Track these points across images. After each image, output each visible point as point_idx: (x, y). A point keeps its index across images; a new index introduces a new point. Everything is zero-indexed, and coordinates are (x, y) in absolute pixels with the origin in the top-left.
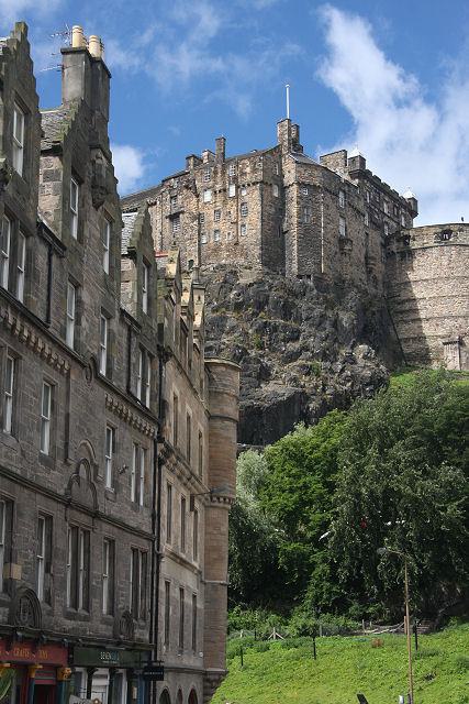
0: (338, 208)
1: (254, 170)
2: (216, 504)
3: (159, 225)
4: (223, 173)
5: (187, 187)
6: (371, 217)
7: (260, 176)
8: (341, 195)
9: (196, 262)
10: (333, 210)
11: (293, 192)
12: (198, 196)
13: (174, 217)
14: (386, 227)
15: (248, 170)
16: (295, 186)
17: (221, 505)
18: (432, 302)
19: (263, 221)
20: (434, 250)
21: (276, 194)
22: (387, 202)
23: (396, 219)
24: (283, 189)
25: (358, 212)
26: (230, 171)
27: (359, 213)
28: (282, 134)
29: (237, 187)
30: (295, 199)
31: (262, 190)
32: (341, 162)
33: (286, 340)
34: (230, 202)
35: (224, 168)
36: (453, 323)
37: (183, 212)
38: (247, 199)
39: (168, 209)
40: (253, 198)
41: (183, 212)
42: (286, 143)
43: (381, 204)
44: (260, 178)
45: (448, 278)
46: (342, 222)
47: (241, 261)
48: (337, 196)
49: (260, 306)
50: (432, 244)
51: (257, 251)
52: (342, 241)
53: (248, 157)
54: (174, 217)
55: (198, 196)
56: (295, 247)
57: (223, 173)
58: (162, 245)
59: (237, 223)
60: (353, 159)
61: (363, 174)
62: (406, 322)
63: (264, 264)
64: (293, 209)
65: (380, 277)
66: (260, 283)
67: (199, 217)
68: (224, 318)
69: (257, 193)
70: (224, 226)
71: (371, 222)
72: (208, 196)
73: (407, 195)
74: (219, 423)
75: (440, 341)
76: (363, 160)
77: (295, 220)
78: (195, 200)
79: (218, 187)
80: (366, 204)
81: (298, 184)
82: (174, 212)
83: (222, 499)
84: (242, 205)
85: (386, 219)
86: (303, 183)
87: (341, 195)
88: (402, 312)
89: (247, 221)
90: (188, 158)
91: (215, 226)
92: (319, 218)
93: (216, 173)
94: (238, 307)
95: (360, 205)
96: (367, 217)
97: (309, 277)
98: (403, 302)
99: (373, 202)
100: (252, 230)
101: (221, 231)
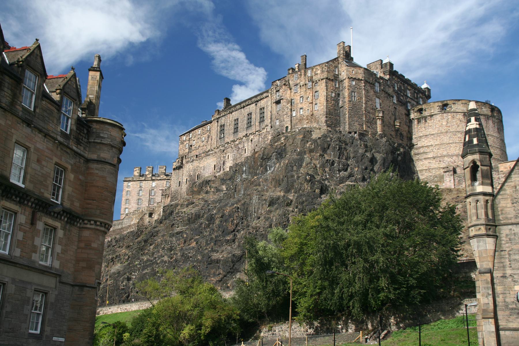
0: (375, 92)
1: (322, 72)
2: (88, 226)
3: (269, 108)
4: (305, 75)
5: (284, 84)
6: (398, 98)
7: (325, 75)
8: (377, 84)
9: (290, 128)
10: (372, 93)
11: (346, 83)
12: (291, 89)
13: (278, 102)
14: (409, 104)
15: (319, 72)
16: (347, 80)
17: (93, 227)
18: (437, 147)
19: (327, 101)
20: (438, 116)
22: (410, 90)
23: (416, 100)
25: (389, 95)
26: (309, 73)
27: (390, 96)
28: (340, 51)
30: (347, 87)
31: (326, 83)
32: (379, 67)
33: (340, 171)
34: (308, 91)
36: (449, 160)
37: (282, 99)
40: (322, 88)
41: (282, 99)
42: (342, 56)
43: (405, 91)
44: (325, 76)
45: (447, 132)
46: (378, 101)
47: (315, 125)
48: (374, 85)
49: (324, 150)
50: (436, 112)
51: (323, 119)
53: (319, 65)
54: (278, 102)
55: (291, 89)
56: (347, 116)
57: (305, 75)
58: (271, 119)
59: (312, 103)
60: (386, 64)
61: (393, 73)
62: (421, 160)
63: (328, 126)
65: (405, 134)
66: (325, 136)
67: (291, 102)
70: (305, 106)
71: (398, 101)
73: (424, 86)
74: (94, 166)
75: (442, 171)
76: (391, 65)
77: (347, 100)
78: (289, 91)
79: (302, 83)
80: (394, 90)
81: (348, 78)
82: (277, 100)
83: (98, 223)
84: (316, 92)
85: (408, 100)
86: (351, 78)
87: (377, 84)
88: (418, 154)
89: (318, 101)
90: (289, 70)
91: (300, 106)
92: (361, 98)
94: (311, 151)
95: (390, 91)
96: (395, 98)
97: (355, 133)
98: (420, 148)
99: (400, 89)
100: (321, 107)
101: (303, 109)
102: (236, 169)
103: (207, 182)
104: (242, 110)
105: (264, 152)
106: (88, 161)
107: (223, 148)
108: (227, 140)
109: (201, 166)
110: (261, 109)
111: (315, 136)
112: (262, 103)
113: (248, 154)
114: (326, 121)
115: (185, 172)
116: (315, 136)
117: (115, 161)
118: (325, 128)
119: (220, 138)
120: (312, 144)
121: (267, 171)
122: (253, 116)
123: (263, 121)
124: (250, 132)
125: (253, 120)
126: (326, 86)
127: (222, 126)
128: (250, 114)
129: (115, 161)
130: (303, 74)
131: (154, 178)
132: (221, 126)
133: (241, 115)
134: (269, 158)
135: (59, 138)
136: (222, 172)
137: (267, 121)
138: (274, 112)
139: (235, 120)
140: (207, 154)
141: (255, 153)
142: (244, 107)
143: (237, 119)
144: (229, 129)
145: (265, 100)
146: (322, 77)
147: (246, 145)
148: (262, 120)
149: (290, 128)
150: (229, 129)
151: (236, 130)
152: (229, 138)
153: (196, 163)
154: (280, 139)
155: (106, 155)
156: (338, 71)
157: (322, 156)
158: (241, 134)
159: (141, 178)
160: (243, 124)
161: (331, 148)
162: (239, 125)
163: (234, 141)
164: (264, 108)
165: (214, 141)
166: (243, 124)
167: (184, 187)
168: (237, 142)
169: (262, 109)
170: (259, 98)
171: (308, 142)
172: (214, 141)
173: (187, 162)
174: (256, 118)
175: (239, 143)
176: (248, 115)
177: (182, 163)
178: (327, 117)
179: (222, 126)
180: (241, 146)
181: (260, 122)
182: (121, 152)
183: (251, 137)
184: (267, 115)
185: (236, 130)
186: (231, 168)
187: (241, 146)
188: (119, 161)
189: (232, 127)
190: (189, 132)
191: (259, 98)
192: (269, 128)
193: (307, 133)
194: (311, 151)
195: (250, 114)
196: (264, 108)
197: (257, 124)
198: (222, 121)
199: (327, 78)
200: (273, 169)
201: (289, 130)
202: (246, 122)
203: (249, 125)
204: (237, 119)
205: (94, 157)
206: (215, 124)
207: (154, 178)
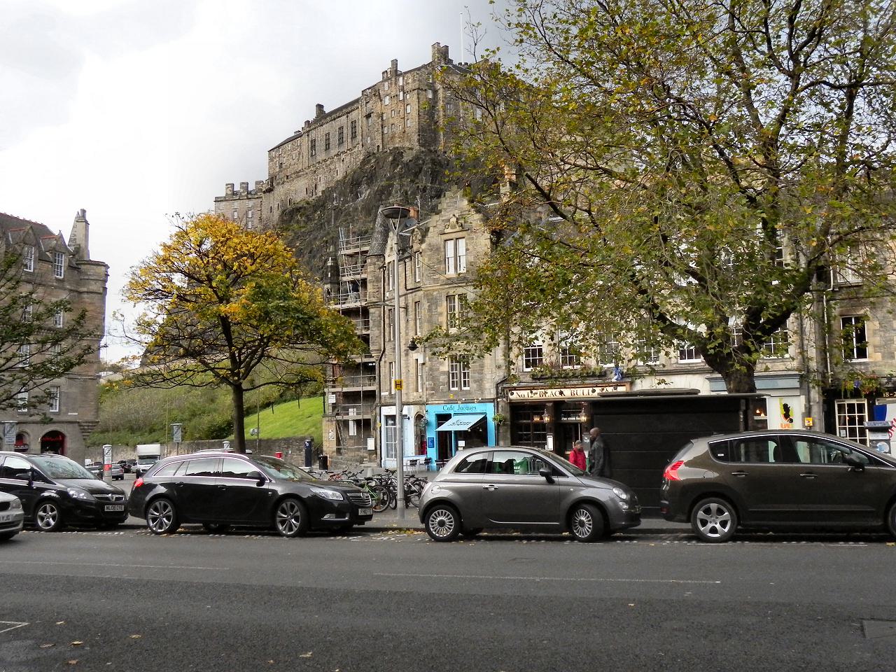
1: (414, 81)
4: (396, 84)
7: (416, 85)
9: (381, 147)
11: (441, 94)
12: (381, 101)
13: (368, 116)
15: (410, 81)
21: (430, 96)
24: (435, 92)
26: (401, 82)
29: (404, 93)
31: (418, 94)
33: (432, 198)
34: (400, 104)
35: (396, 81)
38: (409, 102)
39: (365, 111)
49: (416, 175)
51: (416, 137)
52: (478, 125)
54: (368, 116)
55: (381, 101)
57: (396, 84)
63: (421, 145)
64: (441, 103)
66: (417, 158)
68: (392, 185)
69: (416, 96)
72: (387, 100)
77: (441, 113)
79: (393, 94)
89: (410, 116)
91: (391, 121)
92: (458, 111)
93: (391, 84)
100: (413, 124)
102: (328, 193)
103: (298, 210)
104: (333, 122)
105: (353, 177)
106: (80, 293)
107: (314, 169)
108: (319, 158)
109: (292, 188)
110: (352, 122)
111: (406, 158)
112: (354, 115)
113: (340, 176)
114: (419, 140)
115: (276, 195)
116: (406, 158)
117: (101, 291)
118: (418, 148)
119: (312, 156)
120: (402, 168)
121: (358, 198)
122: (345, 131)
123: (356, 136)
124: (341, 150)
125: (345, 135)
126: (418, 98)
127: (313, 141)
128: (341, 128)
129: (101, 291)
130: (393, 82)
131: (250, 196)
132: (312, 141)
133: (330, 128)
134: (359, 184)
135: (55, 284)
136: (314, 197)
137: (359, 138)
138: (365, 128)
139: (326, 135)
140: (298, 174)
141: (345, 177)
142: (334, 119)
143: (329, 133)
144: (320, 145)
145: (356, 111)
146: (414, 88)
147: (337, 166)
148: (354, 136)
149: (381, 147)
150: (320, 145)
151: (328, 147)
152: (321, 156)
153: (287, 186)
154: (370, 160)
155: (94, 287)
156: (433, 79)
157: (412, 181)
158: (333, 152)
159: (235, 197)
160: (334, 140)
161: (423, 172)
162: (331, 140)
163: (325, 161)
164: (355, 121)
165: (305, 160)
166: (334, 140)
167: (276, 215)
168: (328, 162)
169: (353, 122)
170: (349, 109)
171: (398, 165)
172: (305, 159)
173: (278, 184)
174: (347, 132)
175: (331, 163)
176: (340, 129)
177: (272, 185)
178: (419, 135)
179: (313, 141)
180: (332, 167)
181: (352, 138)
182: (105, 281)
183: (343, 156)
184: (359, 130)
185: (328, 147)
186: (323, 192)
187: (332, 167)
188: (105, 289)
189: (323, 143)
190: (279, 147)
191: (349, 109)
192: (360, 146)
193: (398, 153)
194: (401, 176)
195: (341, 128)
196: (355, 121)
197: (350, 140)
198: (313, 134)
199: (419, 89)
200: (363, 196)
201: (380, 150)
202: (337, 137)
203: (341, 141)
204: (329, 133)
205: (85, 289)
206: (305, 138)
207: (250, 196)
